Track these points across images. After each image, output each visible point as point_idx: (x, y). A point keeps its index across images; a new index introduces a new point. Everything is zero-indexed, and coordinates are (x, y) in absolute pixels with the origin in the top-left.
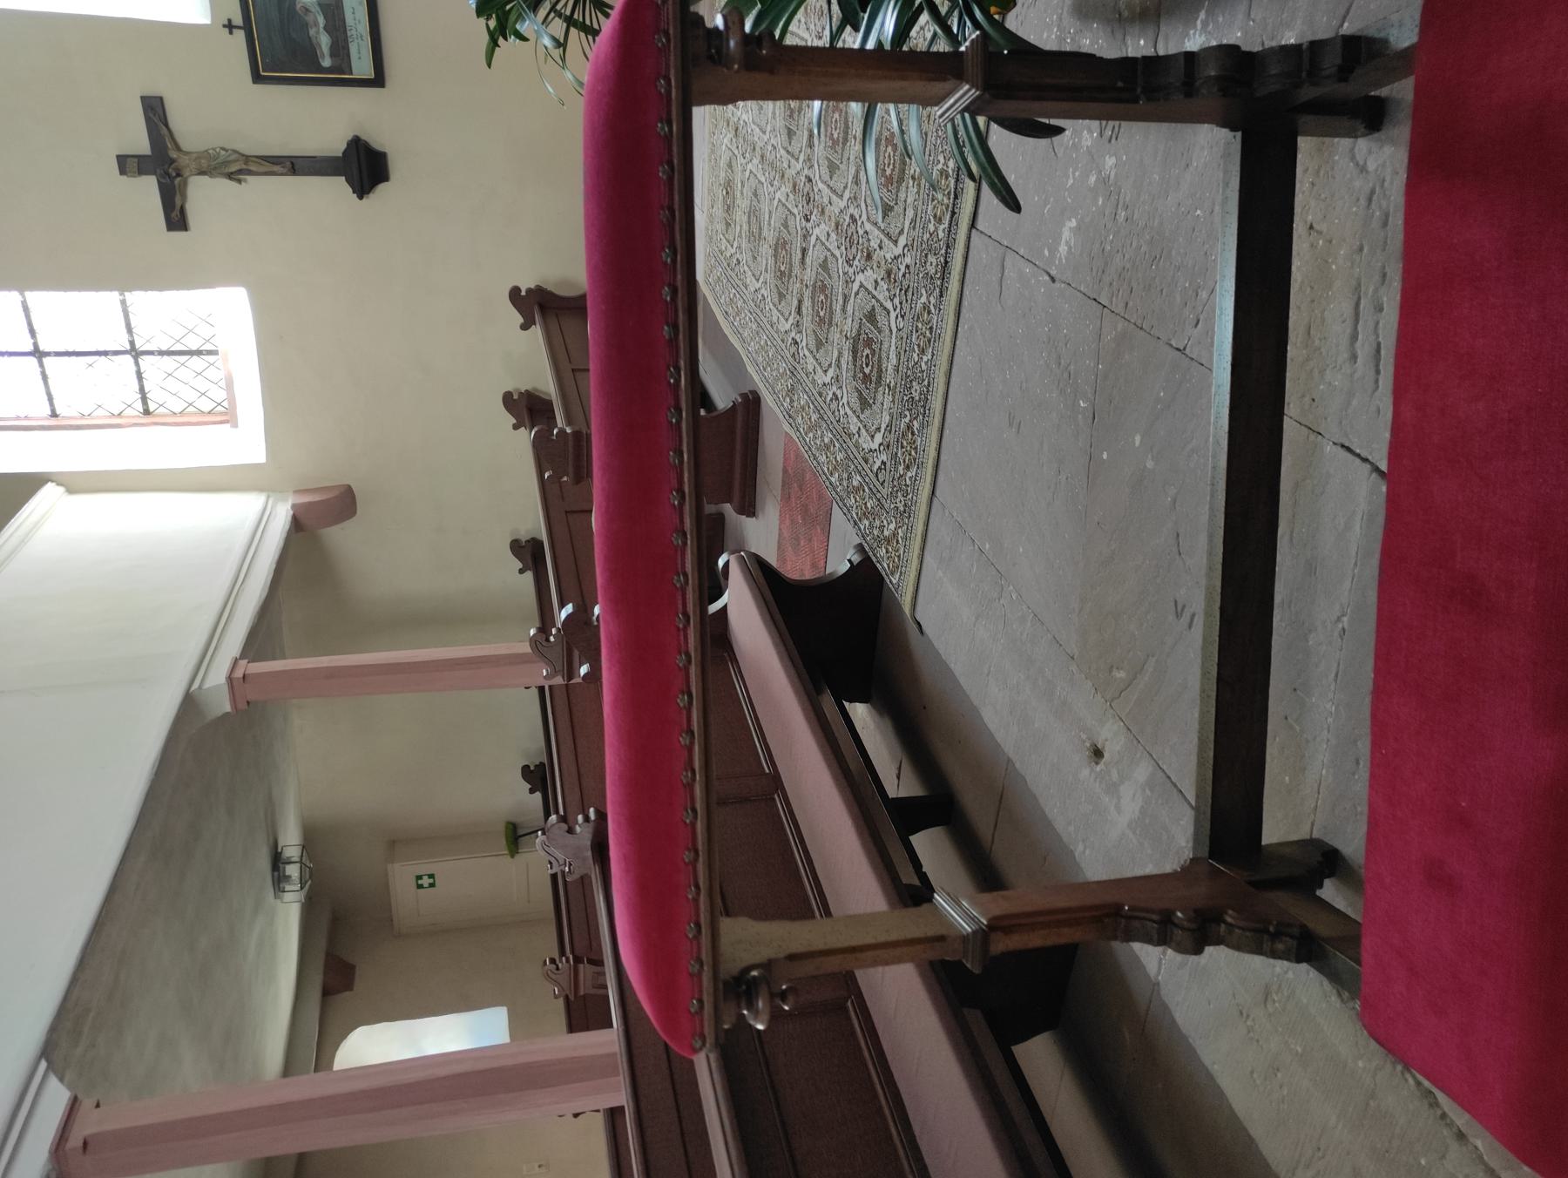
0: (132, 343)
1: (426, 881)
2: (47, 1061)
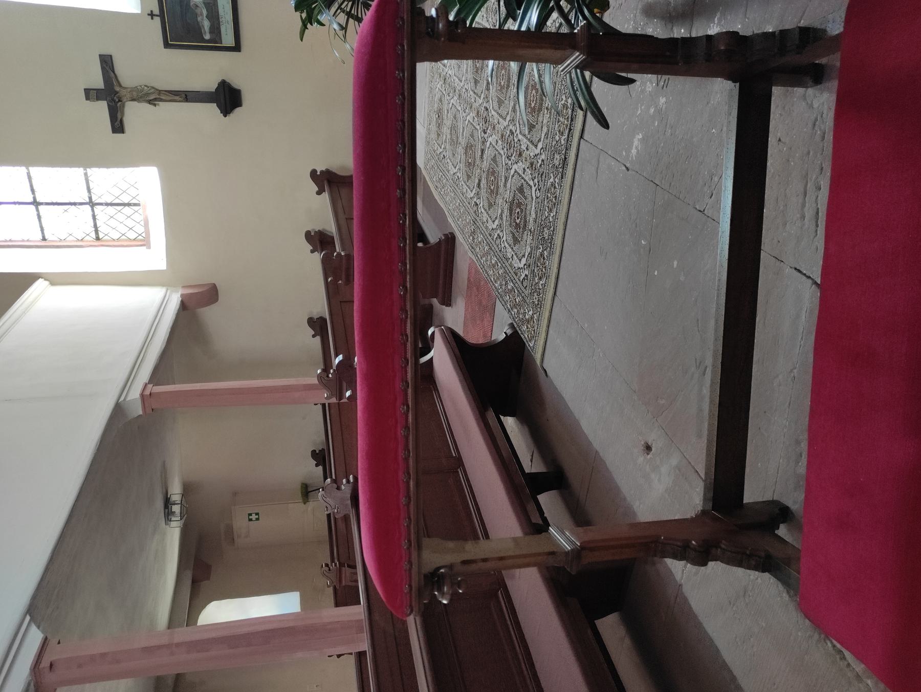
0: (90, 198)
1: (254, 517)
2: (30, 616)
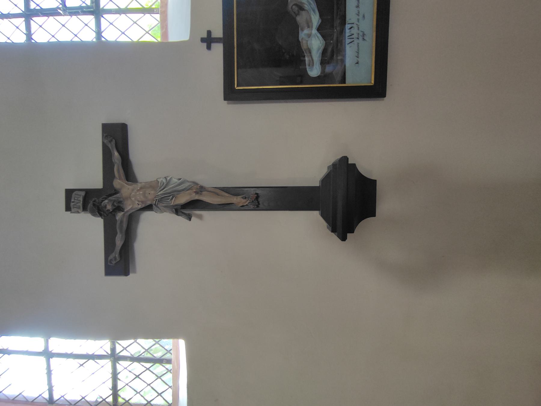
0: (113, 349)
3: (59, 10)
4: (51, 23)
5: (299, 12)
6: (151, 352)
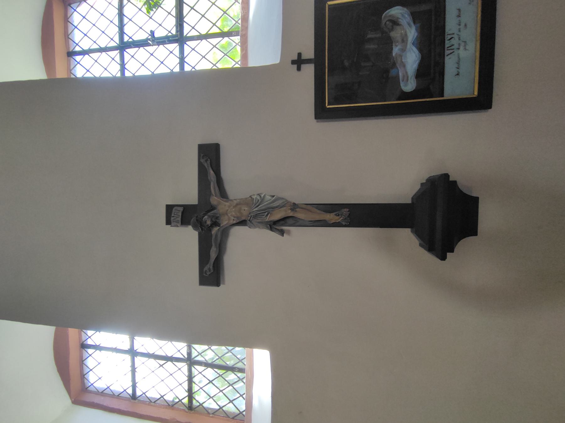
0: (189, 354)
3: (149, 41)
4: (141, 53)
5: (392, 26)
6: (224, 360)
